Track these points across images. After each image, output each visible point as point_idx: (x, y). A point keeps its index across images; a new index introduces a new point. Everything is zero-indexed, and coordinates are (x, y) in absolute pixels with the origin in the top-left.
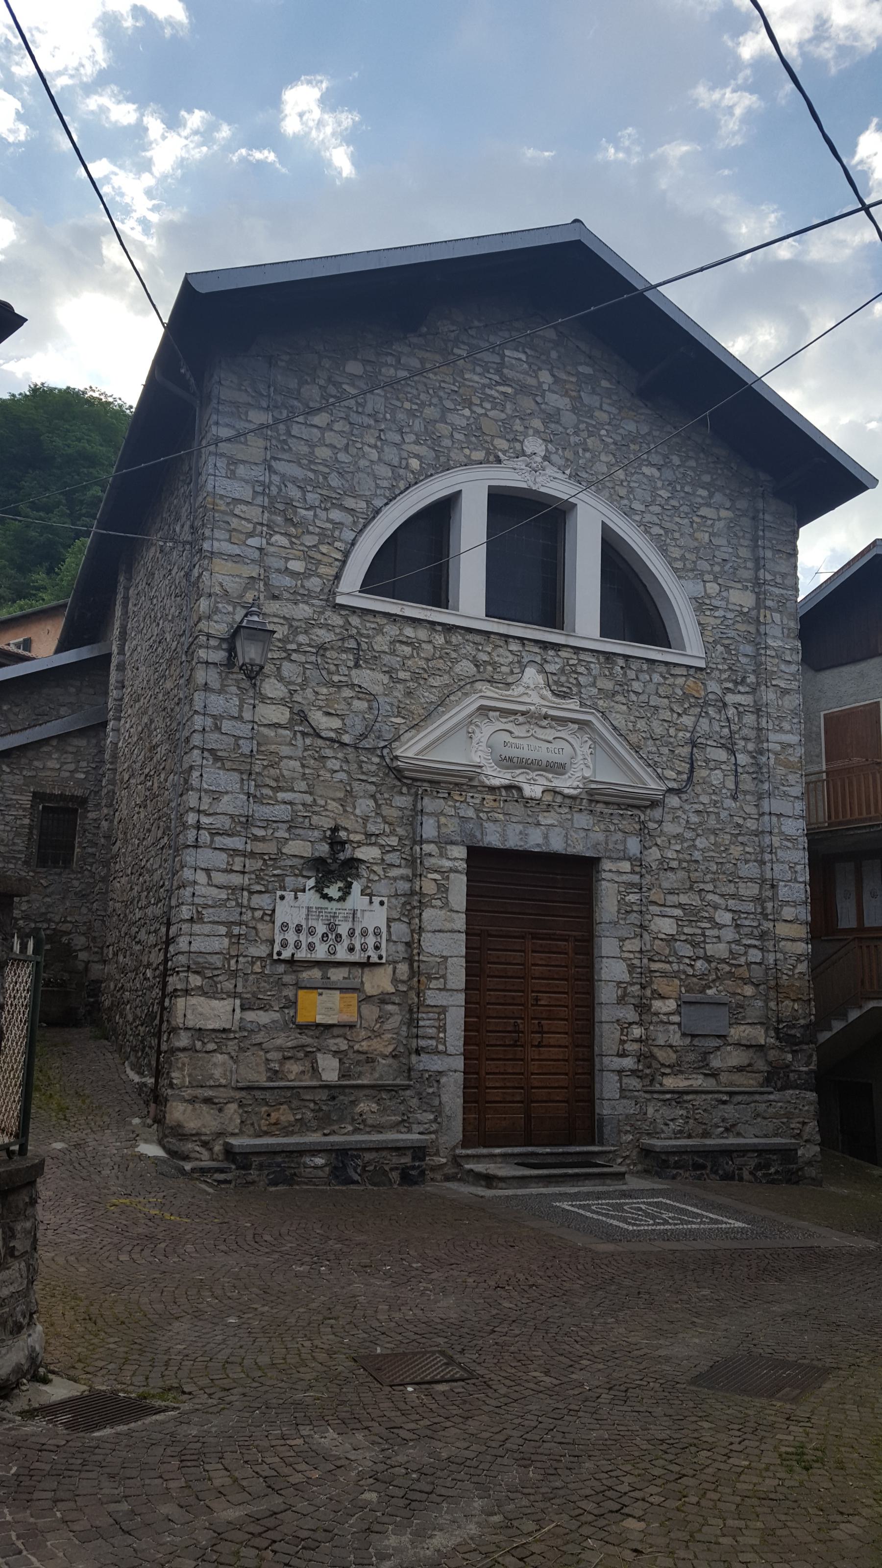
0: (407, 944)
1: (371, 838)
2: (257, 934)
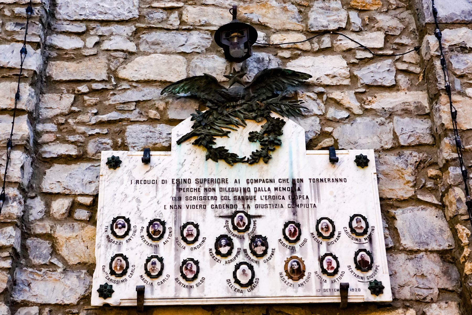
0: (443, 254)
1: (319, 39)
2: (54, 251)
